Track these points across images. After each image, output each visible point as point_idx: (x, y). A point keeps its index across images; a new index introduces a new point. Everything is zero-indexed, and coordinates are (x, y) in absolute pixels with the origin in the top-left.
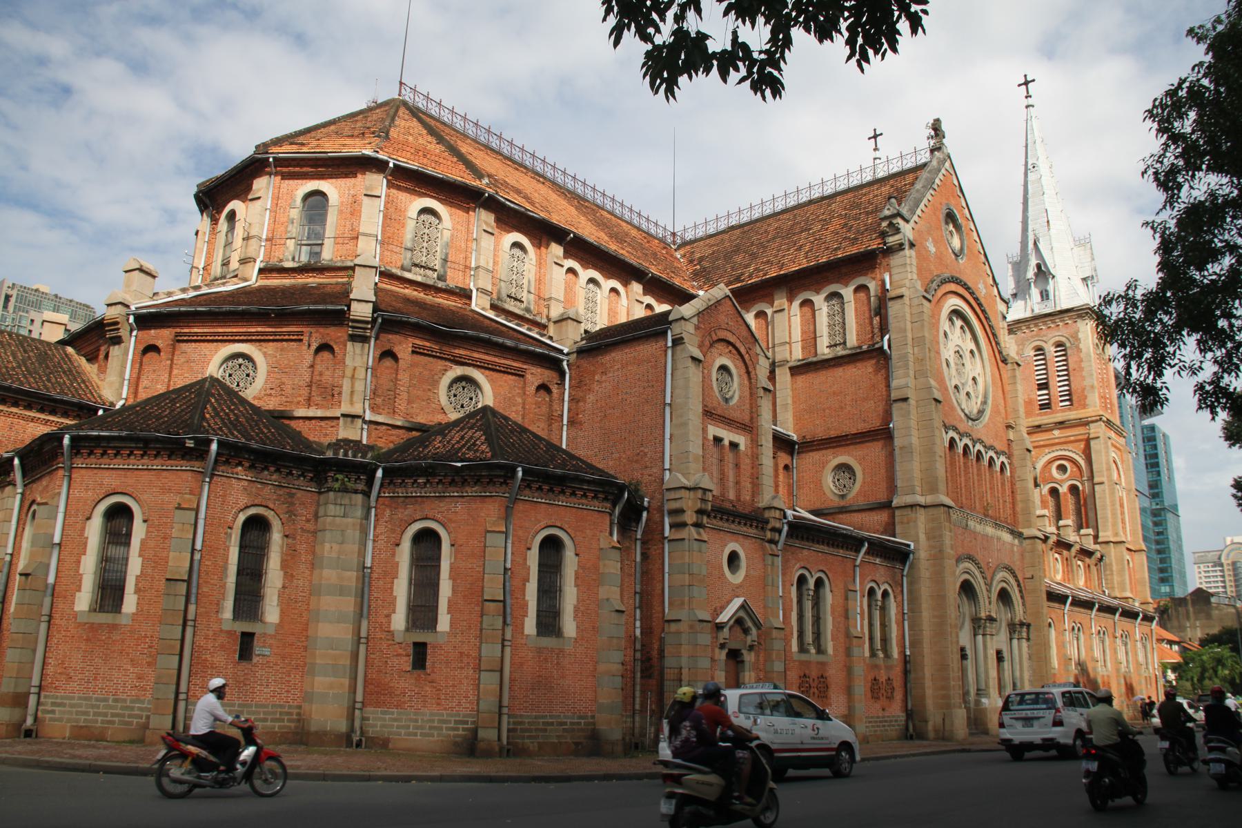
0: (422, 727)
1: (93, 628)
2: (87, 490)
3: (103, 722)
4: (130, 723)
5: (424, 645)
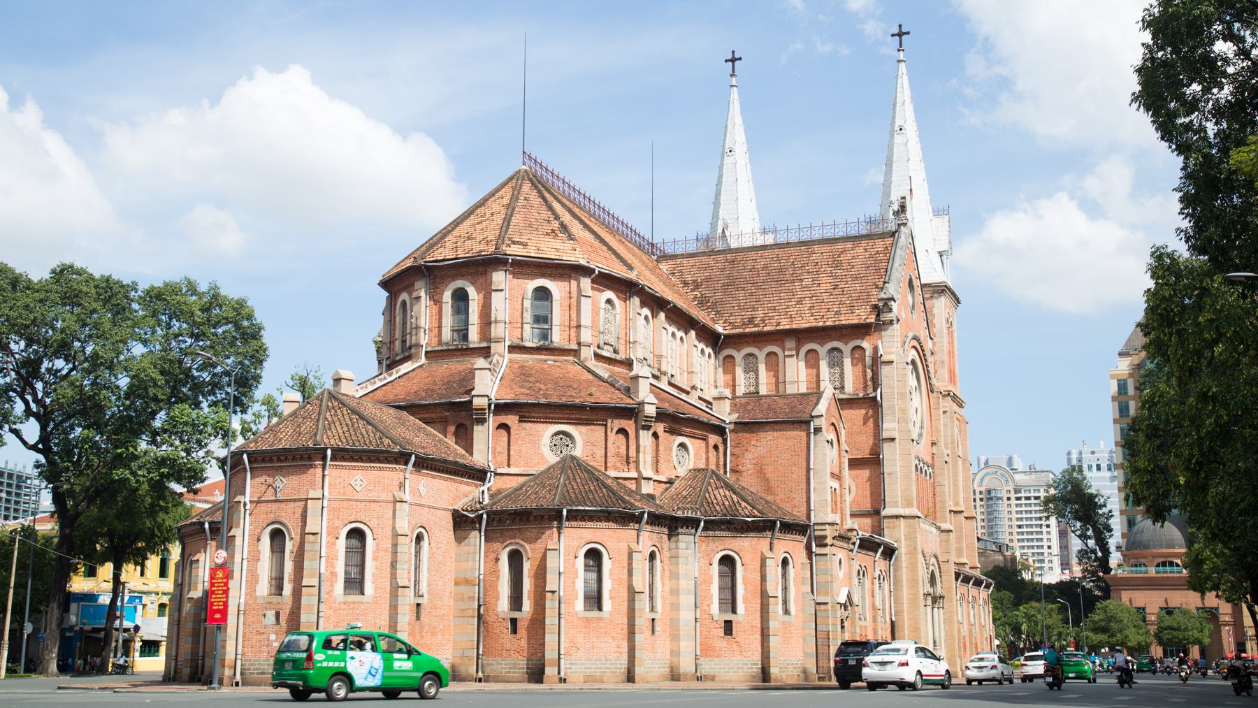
0: (732, 668)
1: (587, 620)
2: (573, 540)
3: (600, 672)
4: (616, 672)
5: (730, 622)
